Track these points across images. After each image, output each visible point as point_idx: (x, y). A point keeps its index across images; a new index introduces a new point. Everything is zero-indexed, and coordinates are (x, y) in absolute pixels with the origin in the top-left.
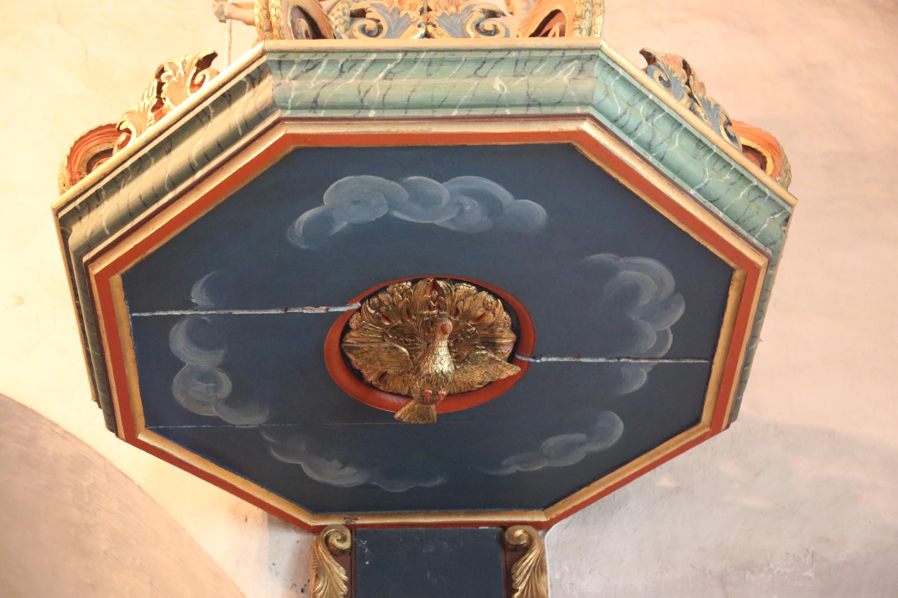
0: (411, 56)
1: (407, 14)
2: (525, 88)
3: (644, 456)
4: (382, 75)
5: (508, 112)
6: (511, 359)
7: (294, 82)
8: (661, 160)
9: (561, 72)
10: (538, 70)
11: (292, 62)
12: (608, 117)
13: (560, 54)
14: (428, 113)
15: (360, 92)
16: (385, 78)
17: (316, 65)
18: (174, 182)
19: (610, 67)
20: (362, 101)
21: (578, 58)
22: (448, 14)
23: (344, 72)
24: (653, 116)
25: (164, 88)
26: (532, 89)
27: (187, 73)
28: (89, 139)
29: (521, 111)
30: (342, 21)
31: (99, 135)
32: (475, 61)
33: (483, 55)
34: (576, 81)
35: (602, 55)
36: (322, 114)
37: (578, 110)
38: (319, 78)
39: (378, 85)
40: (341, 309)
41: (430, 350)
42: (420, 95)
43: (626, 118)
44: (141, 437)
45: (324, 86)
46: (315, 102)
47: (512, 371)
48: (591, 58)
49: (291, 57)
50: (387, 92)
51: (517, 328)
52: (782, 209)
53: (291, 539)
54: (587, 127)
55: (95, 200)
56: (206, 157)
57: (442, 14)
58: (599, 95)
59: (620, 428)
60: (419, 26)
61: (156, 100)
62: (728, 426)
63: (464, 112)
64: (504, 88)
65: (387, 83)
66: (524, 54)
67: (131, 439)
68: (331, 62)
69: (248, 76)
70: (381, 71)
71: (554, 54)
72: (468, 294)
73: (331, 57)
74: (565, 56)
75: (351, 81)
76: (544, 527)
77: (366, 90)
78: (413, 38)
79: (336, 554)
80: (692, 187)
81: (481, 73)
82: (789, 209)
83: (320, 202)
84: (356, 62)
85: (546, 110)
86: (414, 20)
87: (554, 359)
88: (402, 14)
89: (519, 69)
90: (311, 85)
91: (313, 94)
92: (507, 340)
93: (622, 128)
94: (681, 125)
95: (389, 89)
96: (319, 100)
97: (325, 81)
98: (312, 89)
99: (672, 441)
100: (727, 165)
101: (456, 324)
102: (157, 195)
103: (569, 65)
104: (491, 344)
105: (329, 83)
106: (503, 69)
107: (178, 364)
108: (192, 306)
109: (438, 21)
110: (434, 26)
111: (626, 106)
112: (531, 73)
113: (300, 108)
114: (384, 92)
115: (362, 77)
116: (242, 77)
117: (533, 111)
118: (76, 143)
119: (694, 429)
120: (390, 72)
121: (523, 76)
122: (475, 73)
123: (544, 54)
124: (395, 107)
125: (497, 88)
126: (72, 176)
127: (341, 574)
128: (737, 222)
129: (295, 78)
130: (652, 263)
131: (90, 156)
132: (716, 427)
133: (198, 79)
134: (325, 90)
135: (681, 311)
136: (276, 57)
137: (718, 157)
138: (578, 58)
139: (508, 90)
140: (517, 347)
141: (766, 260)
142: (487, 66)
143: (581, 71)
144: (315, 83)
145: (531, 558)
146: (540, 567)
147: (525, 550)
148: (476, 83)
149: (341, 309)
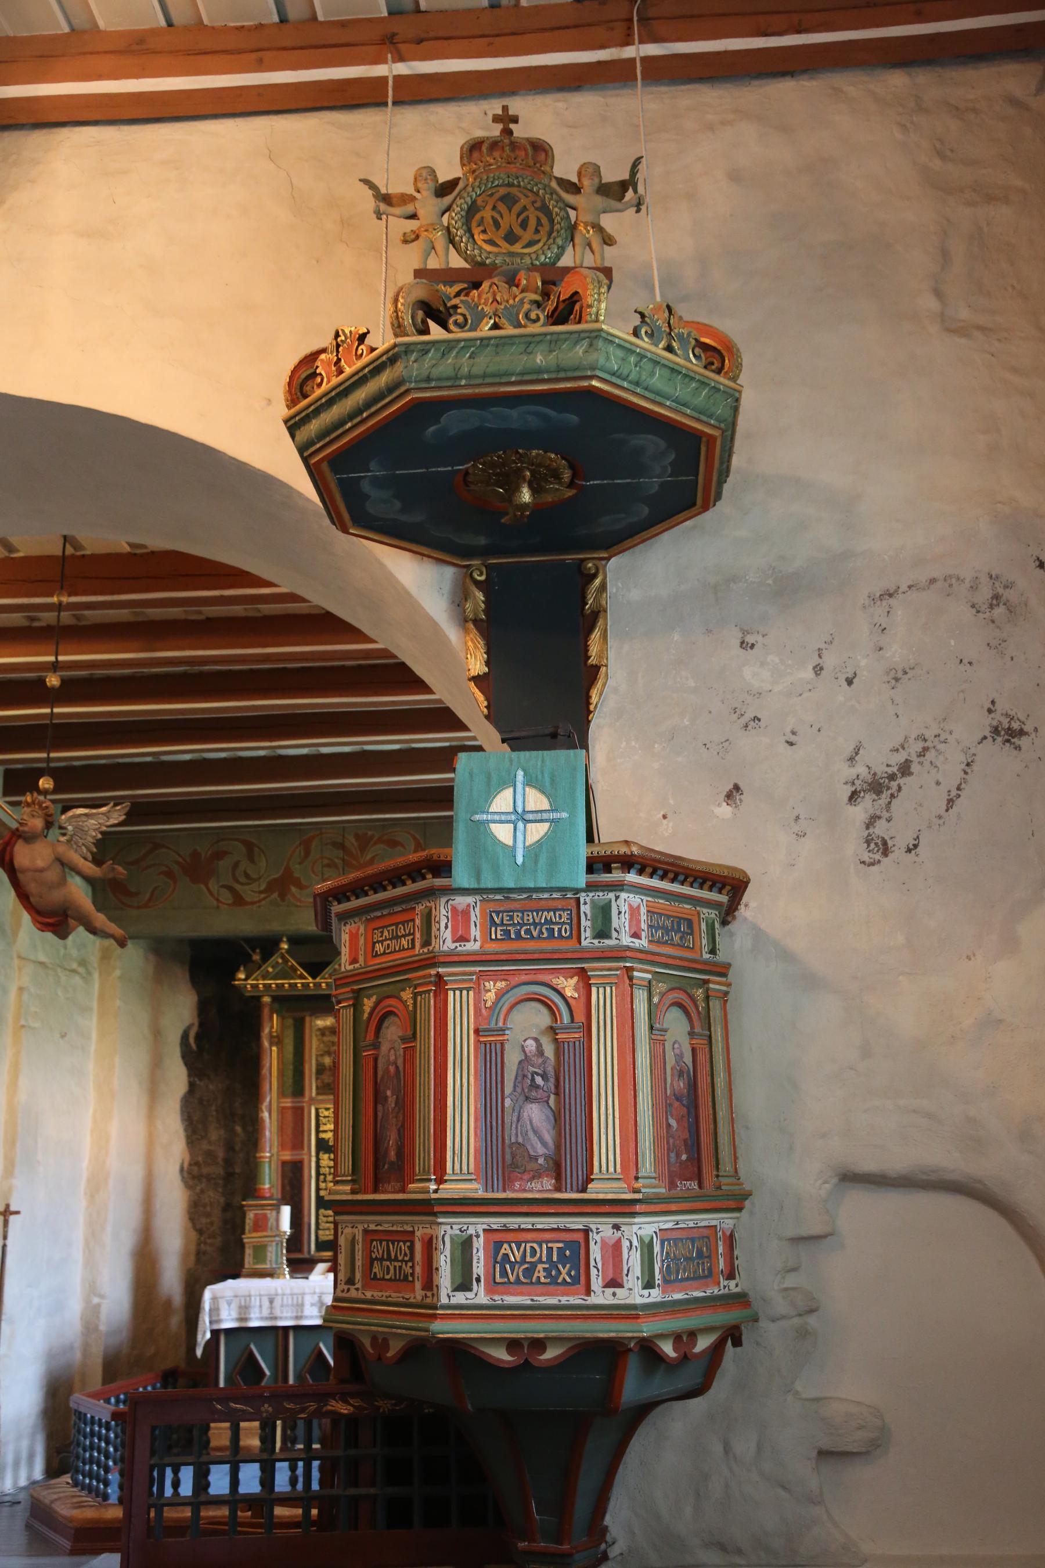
0: (485, 342)
1: (483, 309)
3: (664, 523)
4: (468, 355)
5: (546, 376)
6: (571, 485)
7: (415, 365)
8: (646, 389)
11: (413, 351)
12: (609, 373)
13: (577, 335)
14: (497, 380)
16: (470, 357)
17: (427, 352)
18: (351, 417)
19: (609, 339)
20: (456, 375)
21: (588, 337)
24: (640, 361)
25: (341, 349)
29: (553, 376)
30: (460, 216)
32: (526, 343)
33: (529, 339)
35: (604, 335)
36: (433, 384)
37: (589, 373)
38: (432, 359)
40: (461, 467)
41: (517, 489)
42: (493, 369)
43: (620, 371)
44: (351, 531)
46: (428, 377)
47: (570, 493)
48: (597, 337)
49: (412, 347)
51: (572, 466)
52: (732, 396)
53: (449, 572)
54: (594, 383)
55: (306, 420)
56: (368, 404)
58: (602, 361)
59: (646, 510)
60: (490, 318)
61: (336, 358)
62: (714, 505)
63: (519, 378)
66: (555, 337)
67: (345, 531)
68: (436, 349)
69: (388, 359)
71: (573, 336)
72: (538, 455)
73: (437, 346)
74: (579, 336)
75: (450, 361)
76: (608, 559)
78: (485, 329)
79: (477, 584)
80: (668, 399)
81: (530, 350)
82: (737, 395)
83: (440, 423)
84: (451, 349)
85: (570, 374)
87: (598, 482)
88: (480, 308)
89: (553, 345)
91: (426, 373)
92: (567, 475)
93: (619, 377)
94: (659, 363)
96: (431, 377)
97: (434, 362)
99: (680, 515)
100: (692, 379)
101: (532, 473)
102: (341, 423)
104: (556, 475)
106: (543, 347)
107: (367, 497)
108: (371, 471)
109: (502, 313)
111: (620, 362)
113: (419, 381)
115: (456, 357)
116: (384, 358)
117: (562, 375)
118: (292, 372)
119: (693, 509)
120: (473, 353)
123: (567, 336)
124: (477, 377)
125: (538, 361)
127: (480, 596)
128: (700, 413)
129: (415, 361)
130: (650, 437)
131: (300, 380)
132: (706, 508)
133: (360, 352)
134: (434, 370)
135: (673, 456)
136: (403, 349)
137: (686, 375)
138: (588, 337)
139: (546, 362)
140: (574, 476)
141: (720, 431)
142: (532, 345)
143: (591, 345)
145: (597, 582)
146: (603, 587)
147: (594, 576)
149: (461, 467)
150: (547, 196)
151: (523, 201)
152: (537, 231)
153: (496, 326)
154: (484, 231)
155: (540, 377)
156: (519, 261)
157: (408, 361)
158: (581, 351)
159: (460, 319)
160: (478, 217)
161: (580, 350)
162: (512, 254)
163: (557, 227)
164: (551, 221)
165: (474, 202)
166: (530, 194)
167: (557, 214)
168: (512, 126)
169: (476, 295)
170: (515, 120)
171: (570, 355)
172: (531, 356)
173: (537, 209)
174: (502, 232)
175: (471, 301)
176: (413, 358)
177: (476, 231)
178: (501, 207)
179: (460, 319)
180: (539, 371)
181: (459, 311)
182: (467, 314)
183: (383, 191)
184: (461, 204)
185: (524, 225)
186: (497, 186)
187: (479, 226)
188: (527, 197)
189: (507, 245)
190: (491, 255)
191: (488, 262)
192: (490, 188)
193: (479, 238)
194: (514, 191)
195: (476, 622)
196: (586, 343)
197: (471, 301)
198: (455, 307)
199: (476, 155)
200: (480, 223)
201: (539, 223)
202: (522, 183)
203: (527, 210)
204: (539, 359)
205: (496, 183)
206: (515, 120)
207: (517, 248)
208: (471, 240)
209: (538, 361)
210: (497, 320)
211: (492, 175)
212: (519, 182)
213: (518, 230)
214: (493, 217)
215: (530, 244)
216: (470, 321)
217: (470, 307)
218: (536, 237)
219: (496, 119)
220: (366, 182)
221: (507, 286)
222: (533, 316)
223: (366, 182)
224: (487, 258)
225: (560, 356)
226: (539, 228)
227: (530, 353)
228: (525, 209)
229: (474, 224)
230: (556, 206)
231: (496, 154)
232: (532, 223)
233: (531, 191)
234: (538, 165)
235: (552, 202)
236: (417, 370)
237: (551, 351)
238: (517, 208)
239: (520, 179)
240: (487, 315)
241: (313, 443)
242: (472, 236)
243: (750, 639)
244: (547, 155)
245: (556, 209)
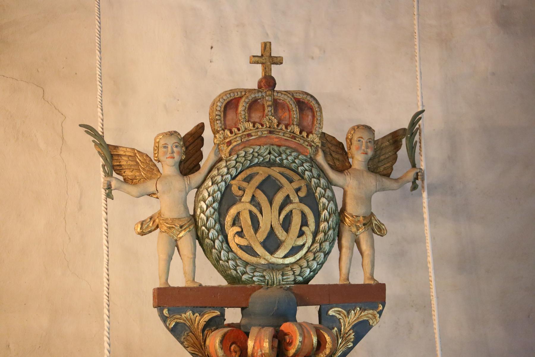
150: (314, 181)
151: (288, 189)
152: (301, 234)
154: (240, 234)
156: (280, 277)
160: (233, 211)
162: (272, 267)
163: (323, 225)
164: (317, 215)
165: (228, 187)
166: (296, 177)
167: (325, 208)
168: (275, 71)
170: (278, 61)
173: (301, 200)
174: (262, 234)
177: (231, 232)
178: (262, 198)
183: (109, 140)
184: (214, 192)
185: (286, 225)
186: (258, 165)
187: (234, 224)
188: (291, 181)
189: (268, 256)
190: (248, 269)
191: (245, 277)
192: (248, 167)
193: (234, 241)
194: (275, 172)
199: (231, 115)
200: (236, 221)
201: (304, 223)
202: (285, 161)
203: (291, 202)
205: (256, 160)
206: (278, 61)
207: (278, 258)
208: (225, 245)
211: (251, 151)
212: (282, 160)
213: (280, 233)
214: (250, 212)
215: (294, 250)
218: (300, 242)
219: (255, 60)
220: (90, 130)
223: (90, 130)
224: (244, 273)
226: (304, 229)
228: (287, 201)
229: (229, 220)
230: (324, 196)
231: (256, 116)
232: (296, 221)
233: (298, 173)
234: (304, 134)
235: (319, 189)
238: (279, 198)
239: (284, 156)
242: (226, 237)
244: (314, 116)
245: (323, 200)
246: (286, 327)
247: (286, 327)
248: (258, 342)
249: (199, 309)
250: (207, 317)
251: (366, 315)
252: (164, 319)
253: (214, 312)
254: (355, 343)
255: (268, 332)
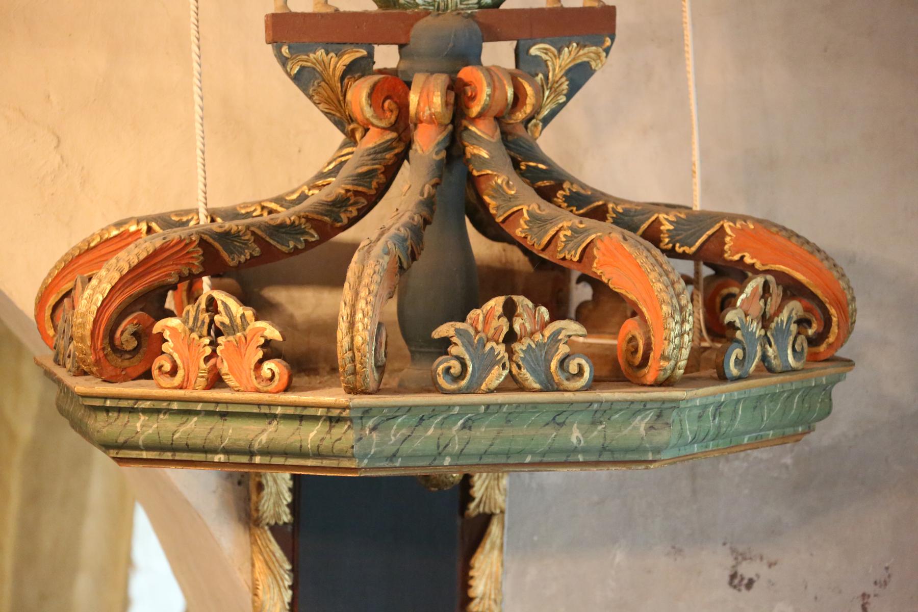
2: (602, 441)
4: (461, 422)
7: (374, 435)
9: (639, 418)
10: (617, 416)
15: (438, 447)
16: (464, 427)
22: (534, 346)
23: (424, 420)
26: (608, 442)
27: (248, 339)
28: (112, 297)
31: (119, 289)
34: (653, 431)
39: (457, 438)
45: (404, 441)
50: (465, 447)
57: (528, 347)
63: (537, 459)
64: (580, 441)
65: (466, 434)
70: (461, 419)
77: (444, 445)
81: (560, 419)
86: (499, 357)
90: (391, 440)
91: (394, 449)
95: (468, 443)
97: (404, 431)
98: (392, 445)
103: (648, 412)
105: (409, 436)
110: (519, 367)
112: (609, 419)
114: (462, 447)
121: (601, 423)
122: (554, 419)
125: (574, 440)
126: (96, 355)
129: (374, 429)
134: (405, 446)
139: (585, 442)
143: (659, 416)
144: (395, 435)
148: (553, 436)
153: (513, 384)
155: (571, 459)
157: (363, 428)
158: (642, 429)
159: (456, 368)
161: (641, 424)
169: (481, 318)
171: (626, 432)
172: (563, 431)
175: (472, 332)
176: (371, 423)
179: (456, 368)
180: (575, 450)
181: (453, 350)
182: (467, 357)
195: (277, 530)
196: (651, 415)
197: (472, 332)
198: (446, 342)
204: (575, 436)
209: (574, 440)
210: (515, 370)
216: (470, 369)
217: (471, 343)
221: (530, 304)
222: (573, 368)
225: (609, 432)
227: (561, 425)
236: (377, 446)
237: (594, 423)
240: (497, 363)
241: (136, 448)
243: (747, 570)
246: (466, 73)
247: (466, 73)
248: (426, 97)
249: (336, 46)
250: (347, 59)
251: (587, 53)
252: (284, 61)
253: (358, 52)
254: (569, 96)
255: (441, 80)
